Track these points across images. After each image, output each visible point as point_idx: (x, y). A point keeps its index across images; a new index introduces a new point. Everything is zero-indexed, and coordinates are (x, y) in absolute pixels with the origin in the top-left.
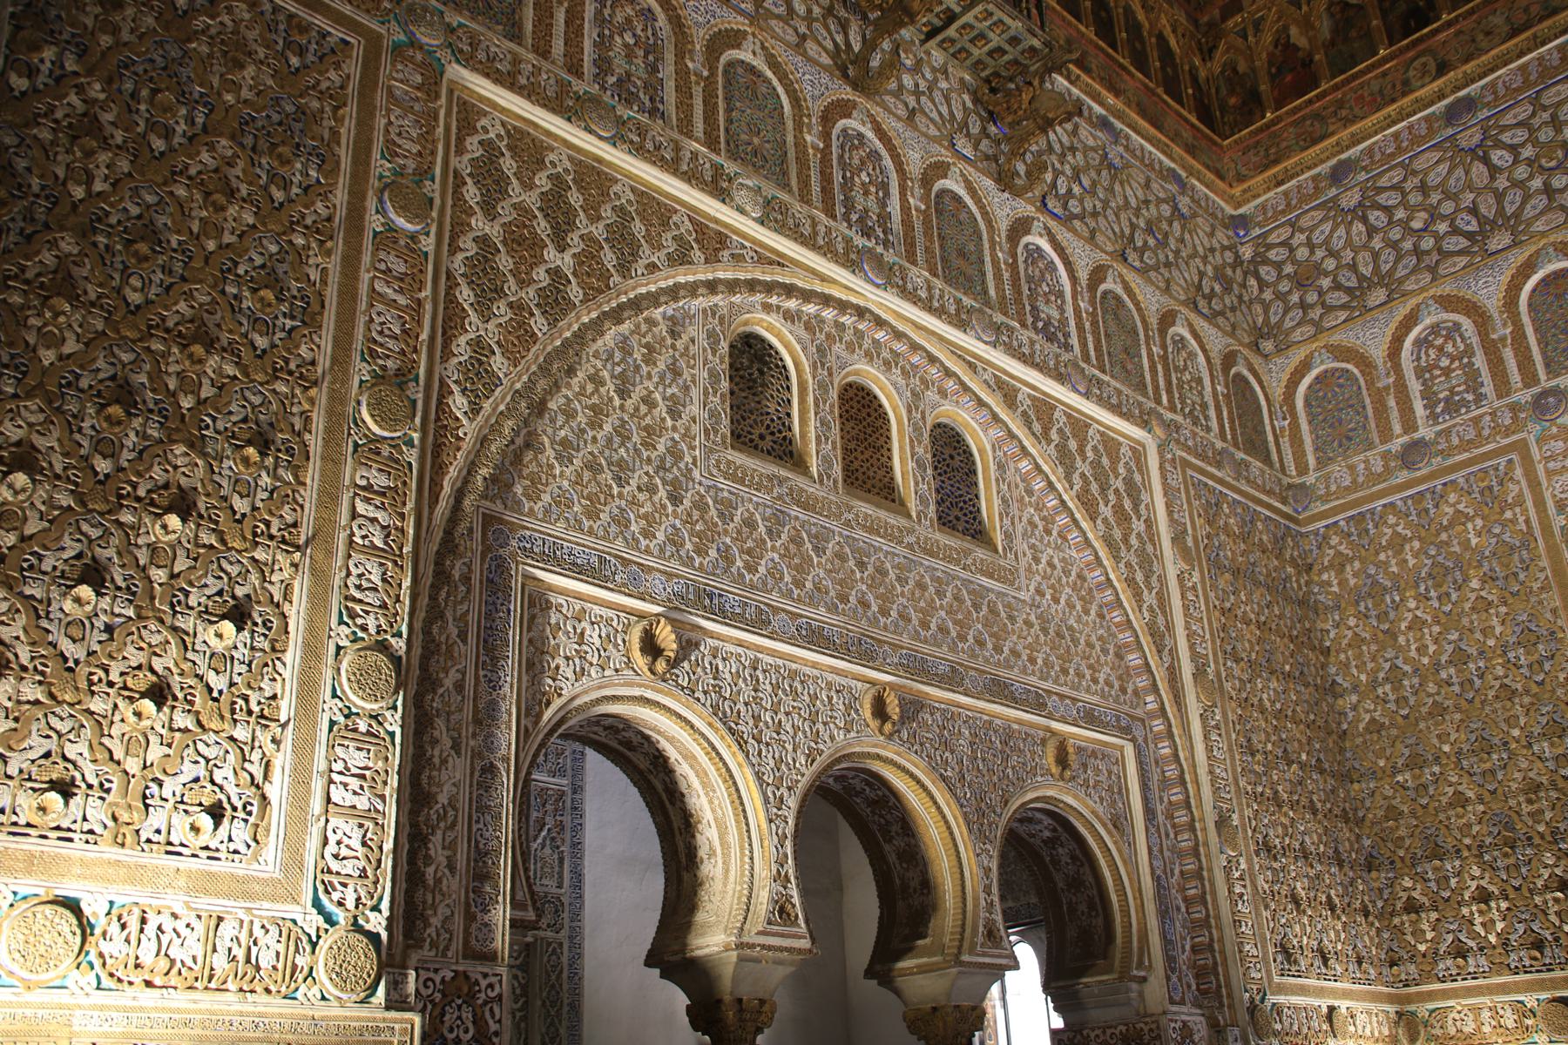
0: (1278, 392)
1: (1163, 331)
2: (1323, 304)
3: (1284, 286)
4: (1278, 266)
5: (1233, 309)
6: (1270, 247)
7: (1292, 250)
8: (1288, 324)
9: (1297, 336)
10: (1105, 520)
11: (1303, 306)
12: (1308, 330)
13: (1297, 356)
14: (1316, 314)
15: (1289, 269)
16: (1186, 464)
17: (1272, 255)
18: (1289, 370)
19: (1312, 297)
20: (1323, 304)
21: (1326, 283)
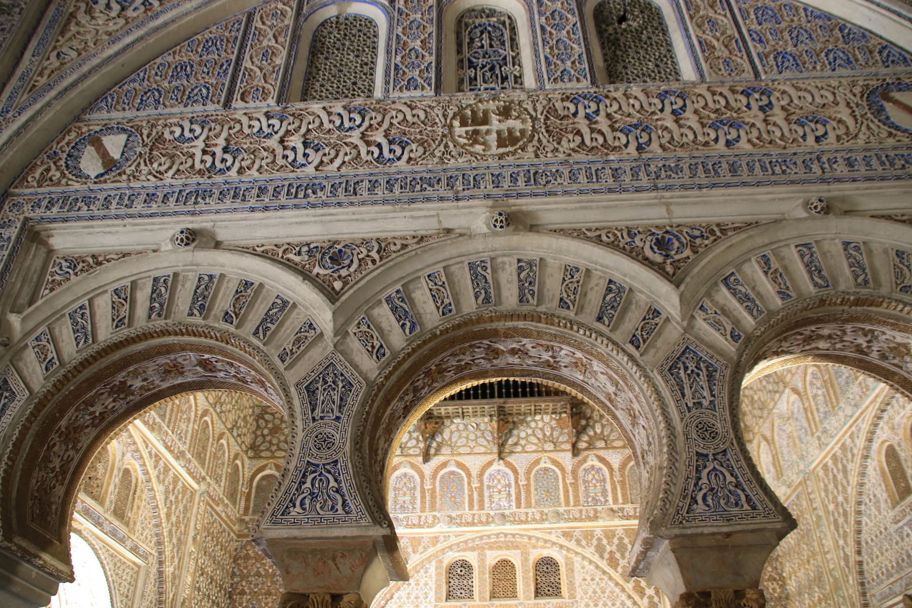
0: (248, 475)
1: (218, 440)
2: (278, 446)
3: (266, 432)
4: (267, 422)
5: (245, 435)
6: (267, 413)
7: (274, 418)
8: (262, 448)
9: (263, 454)
10: (172, 523)
11: (270, 442)
12: (268, 454)
13: (263, 462)
14: (274, 448)
15: (270, 425)
16: (208, 504)
17: (267, 417)
18: (257, 467)
19: (275, 441)
20: (278, 446)
21: (282, 438)
